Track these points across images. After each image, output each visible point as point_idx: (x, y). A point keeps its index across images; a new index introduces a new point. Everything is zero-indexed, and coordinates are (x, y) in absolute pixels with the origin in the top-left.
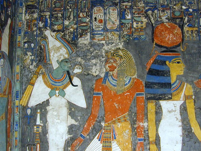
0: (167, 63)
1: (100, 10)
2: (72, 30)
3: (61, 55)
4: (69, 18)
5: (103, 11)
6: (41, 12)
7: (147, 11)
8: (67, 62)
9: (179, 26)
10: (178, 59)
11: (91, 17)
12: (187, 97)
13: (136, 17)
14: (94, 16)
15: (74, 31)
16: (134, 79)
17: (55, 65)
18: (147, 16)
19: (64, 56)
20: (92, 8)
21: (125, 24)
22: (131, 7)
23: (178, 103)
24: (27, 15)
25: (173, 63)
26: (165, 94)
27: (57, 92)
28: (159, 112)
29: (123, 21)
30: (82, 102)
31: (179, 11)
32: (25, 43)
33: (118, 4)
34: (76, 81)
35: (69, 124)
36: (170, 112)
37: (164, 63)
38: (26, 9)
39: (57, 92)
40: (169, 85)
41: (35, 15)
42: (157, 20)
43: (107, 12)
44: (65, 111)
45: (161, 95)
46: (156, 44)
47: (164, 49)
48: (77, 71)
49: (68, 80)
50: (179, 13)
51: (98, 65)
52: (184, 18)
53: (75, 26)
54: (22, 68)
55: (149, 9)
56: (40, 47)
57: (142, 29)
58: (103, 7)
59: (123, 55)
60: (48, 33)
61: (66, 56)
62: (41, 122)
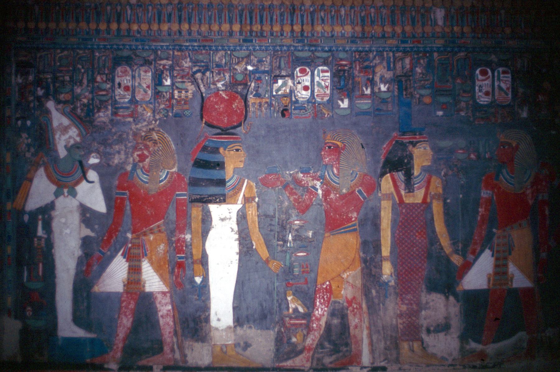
0: (221, 150)
1: (126, 71)
3: (70, 137)
4: (81, 82)
5: (130, 73)
7: (195, 73)
8: (78, 148)
9: (242, 95)
11: (113, 81)
12: (247, 200)
14: (117, 80)
15: (88, 102)
16: (172, 173)
17: (62, 153)
18: (195, 82)
19: (74, 139)
22: (172, 68)
25: (230, 151)
26: (216, 195)
29: (160, 88)
31: (242, 73)
32: (17, 119)
33: (153, 62)
34: (92, 175)
36: (222, 220)
37: (216, 151)
39: (66, 191)
40: (222, 182)
41: (31, 78)
42: (209, 87)
43: (137, 75)
44: (76, 218)
45: (210, 196)
46: (205, 123)
47: (219, 131)
48: (93, 160)
49: (79, 173)
51: (122, 152)
52: (249, 84)
53: (90, 96)
58: (131, 68)
59: (159, 139)
61: (78, 139)
62: (44, 232)
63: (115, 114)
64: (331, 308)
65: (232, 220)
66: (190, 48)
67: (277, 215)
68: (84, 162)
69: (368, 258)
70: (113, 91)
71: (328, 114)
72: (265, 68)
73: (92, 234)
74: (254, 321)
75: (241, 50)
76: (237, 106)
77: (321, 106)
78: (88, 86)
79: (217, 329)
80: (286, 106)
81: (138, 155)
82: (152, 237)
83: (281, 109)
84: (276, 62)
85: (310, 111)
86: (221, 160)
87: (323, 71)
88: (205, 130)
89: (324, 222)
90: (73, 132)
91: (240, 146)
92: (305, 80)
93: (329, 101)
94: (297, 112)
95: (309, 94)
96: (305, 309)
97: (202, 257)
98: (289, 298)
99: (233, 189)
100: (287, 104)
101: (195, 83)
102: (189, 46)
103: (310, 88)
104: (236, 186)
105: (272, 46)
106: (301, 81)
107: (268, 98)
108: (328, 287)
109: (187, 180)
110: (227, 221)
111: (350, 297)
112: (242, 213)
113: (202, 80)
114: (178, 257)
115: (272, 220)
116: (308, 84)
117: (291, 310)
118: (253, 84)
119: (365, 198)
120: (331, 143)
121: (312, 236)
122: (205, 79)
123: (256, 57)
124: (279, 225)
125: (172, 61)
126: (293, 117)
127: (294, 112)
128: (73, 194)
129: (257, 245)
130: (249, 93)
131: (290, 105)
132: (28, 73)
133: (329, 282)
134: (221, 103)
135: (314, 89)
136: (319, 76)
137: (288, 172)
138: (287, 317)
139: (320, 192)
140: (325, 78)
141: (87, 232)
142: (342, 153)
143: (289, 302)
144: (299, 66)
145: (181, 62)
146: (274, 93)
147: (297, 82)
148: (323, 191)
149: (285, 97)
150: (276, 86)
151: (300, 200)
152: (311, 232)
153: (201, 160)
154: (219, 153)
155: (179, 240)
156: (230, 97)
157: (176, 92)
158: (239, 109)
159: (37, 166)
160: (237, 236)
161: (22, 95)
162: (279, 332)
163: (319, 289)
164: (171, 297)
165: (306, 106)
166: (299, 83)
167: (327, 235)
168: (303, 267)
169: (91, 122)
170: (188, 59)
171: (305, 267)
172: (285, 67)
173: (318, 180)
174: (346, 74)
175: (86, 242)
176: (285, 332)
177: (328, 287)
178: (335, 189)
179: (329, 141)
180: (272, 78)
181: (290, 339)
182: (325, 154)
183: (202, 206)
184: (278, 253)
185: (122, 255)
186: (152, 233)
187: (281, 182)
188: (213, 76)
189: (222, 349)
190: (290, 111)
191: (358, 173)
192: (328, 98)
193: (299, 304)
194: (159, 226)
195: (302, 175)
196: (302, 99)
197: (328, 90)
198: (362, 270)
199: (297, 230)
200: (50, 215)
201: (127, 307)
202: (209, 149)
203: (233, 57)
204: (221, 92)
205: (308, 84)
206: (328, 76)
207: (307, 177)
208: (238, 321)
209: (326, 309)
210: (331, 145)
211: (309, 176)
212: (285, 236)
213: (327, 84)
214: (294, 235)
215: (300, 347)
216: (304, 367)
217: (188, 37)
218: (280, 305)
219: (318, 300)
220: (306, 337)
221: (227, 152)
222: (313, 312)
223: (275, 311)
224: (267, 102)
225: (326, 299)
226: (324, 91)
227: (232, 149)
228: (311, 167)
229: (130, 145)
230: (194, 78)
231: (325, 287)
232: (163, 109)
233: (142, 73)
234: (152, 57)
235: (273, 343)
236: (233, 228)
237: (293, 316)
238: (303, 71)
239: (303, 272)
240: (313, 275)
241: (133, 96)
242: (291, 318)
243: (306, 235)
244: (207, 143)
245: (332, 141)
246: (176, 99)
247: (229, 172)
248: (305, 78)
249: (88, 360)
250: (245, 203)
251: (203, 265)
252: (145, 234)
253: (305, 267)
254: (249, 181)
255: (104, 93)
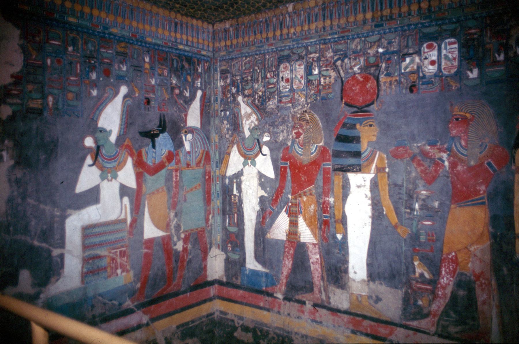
0: (358, 126)
1: (286, 66)
2: (260, 93)
3: (252, 122)
4: (257, 79)
5: (289, 68)
6: (233, 76)
7: (336, 61)
8: (257, 129)
9: (374, 76)
10: (370, 122)
11: (278, 75)
12: (380, 170)
13: (324, 70)
14: (281, 75)
15: (262, 94)
16: (320, 147)
17: (247, 133)
18: (336, 69)
19: (254, 123)
20: (279, 66)
21: (312, 81)
22: (319, 59)
23: (369, 177)
24: (222, 81)
25: (364, 126)
26: (353, 165)
27: (249, 161)
28: (346, 187)
29: (310, 78)
30: (270, 173)
31: (374, 56)
32: (222, 111)
33: (305, 57)
34: (265, 150)
35: (259, 195)
36: (359, 187)
37: (353, 127)
38: (221, 74)
39: (249, 161)
40: (357, 154)
41: (228, 81)
42: (347, 72)
43: (294, 69)
44: (255, 182)
45: (349, 166)
46: (345, 104)
47: (355, 109)
48: (266, 139)
49: (257, 149)
50: (374, 59)
51: (285, 131)
52: (380, 65)
53: (264, 90)
54: (220, 137)
55: (338, 59)
56: (234, 114)
57: (329, 86)
58: (289, 63)
59: (310, 119)
60: (240, 99)
61: (256, 123)
62: (237, 191)
63: (280, 101)
64: (458, 279)
65: (366, 187)
66: (332, 40)
67: (405, 185)
68: (260, 140)
69: (498, 234)
70: (279, 84)
71: (456, 86)
72: (394, 48)
73: (266, 195)
74: (385, 278)
75: (373, 35)
76: (371, 86)
77: (449, 79)
78: (262, 82)
79: (354, 280)
80: (414, 82)
81: (295, 133)
82: (305, 199)
83: (409, 85)
84: (404, 42)
85: (437, 84)
86: (357, 135)
87: (450, 44)
88: (344, 109)
89: (450, 193)
90: (254, 118)
91: (373, 122)
92: (432, 55)
93: (456, 73)
94: (424, 86)
95: (436, 68)
96: (431, 276)
97: (342, 218)
98: (416, 263)
99: (367, 160)
100: (415, 80)
101: (336, 70)
102: (331, 39)
103: (437, 62)
104: (369, 158)
105: (401, 27)
106: (427, 57)
107: (397, 76)
108: (454, 258)
109: (331, 152)
110: (363, 187)
111: (478, 271)
112: (374, 181)
113: (342, 66)
114: (324, 216)
115: (400, 189)
116: (435, 58)
117: (417, 275)
118: (384, 65)
119: (495, 171)
120: (459, 115)
121: (438, 206)
122: (344, 65)
123: (386, 40)
124: (406, 193)
125: (319, 53)
126: (420, 92)
127: (421, 87)
128: (254, 164)
129: (387, 210)
130: (381, 73)
131: (417, 81)
132: (226, 78)
133: (455, 252)
134: (357, 85)
135: (441, 62)
136: (446, 48)
137: (415, 145)
138: (414, 280)
139: (446, 164)
140: (453, 50)
141: (262, 193)
142: (471, 124)
143: (416, 267)
144: (426, 42)
145: (326, 54)
146: (403, 71)
147: (424, 57)
148: (449, 163)
149: (413, 73)
150: (404, 64)
151: (427, 171)
152: (438, 202)
153: (341, 135)
154: (356, 129)
155: (324, 203)
156: (365, 78)
157: (322, 79)
158: (372, 89)
159: (232, 143)
160: (370, 202)
161: (224, 93)
162: (406, 293)
163: (445, 259)
164: (319, 248)
165: (433, 80)
166: (426, 58)
167: (453, 206)
168: (429, 235)
169: (264, 109)
170: (331, 50)
171: (430, 235)
172: (413, 45)
173: (445, 152)
174: (476, 43)
175: (262, 200)
176: (412, 293)
177: (454, 258)
178: (462, 161)
179: (457, 113)
180: (400, 57)
181: (416, 301)
182: (452, 127)
183: (343, 174)
184: (405, 219)
185: (285, 211)
186: (305, 195)
187: (409, 154)
188: (350, 62)
189: (357, 298)
190: (417, 86)
191: (488, 144)
192: (456, 69)
193: (425, 270)
194: (310, 190)
195: (429, 148)
196: (428, 74)
197: (455, 62)
198: (492, 245)
199: (424, 200)
200: (240, 179)
201: (288, 252)
202: (348, 125)
203: (366, 42)
204: (357, 75)
205: (435, 58)
206: (455, 48)
207: (434, 149)
208: (372, 276)
209: (451, 279)
210: (458, 116)
211: (436, 148)
212: (412, 205)
213: (454, 56)
214: (420, 204)
215: (426, 311)
216: (430, 330)
217: (330, 32)
218: (407, 268)
219: (444, 269)
220: (431, 303)
221: (362, 127)
222: (438, 279)
223: (402, 273)
224: (396, 80)
225: (451, 269)
226: (451, 63)
227: (366, 125)
228: (438, 139)
229: (290, 125)
230: (335, 66)
231: (450, 257)
232: (314, 94)
233: (297, 67)
234: (304, 53)
235: (400, 302)
236: (367, 194)
237: (419, 280)
238: (430, 47)
239: (429, 240)
240: (438, 244)
241: (292, 86)
242: (417, 282)
243: (432, 204)
244: (346, 120)
245: (459, 113)
246: (322, 85)
247: (364, 146)
248: (431, 53)
249: (264, 288)
250: (377, 173)
251: (343, 224)
252: (300, 196)
253: (430, 235)
254: (381, 153)
255: (272, 86)
